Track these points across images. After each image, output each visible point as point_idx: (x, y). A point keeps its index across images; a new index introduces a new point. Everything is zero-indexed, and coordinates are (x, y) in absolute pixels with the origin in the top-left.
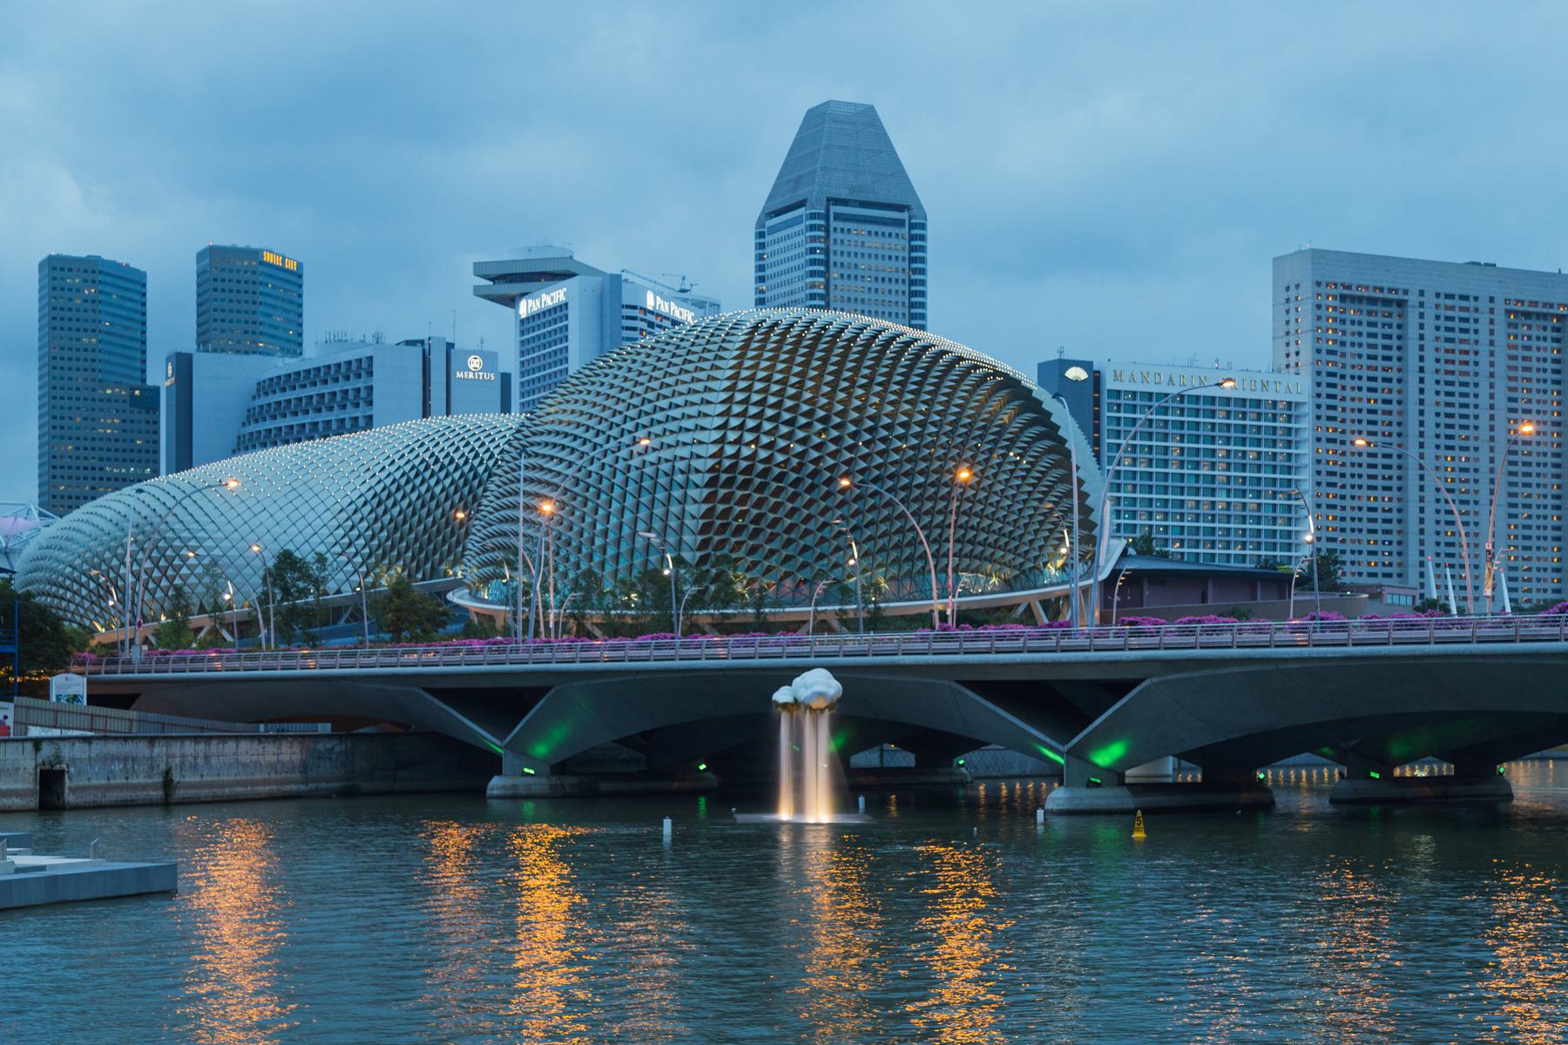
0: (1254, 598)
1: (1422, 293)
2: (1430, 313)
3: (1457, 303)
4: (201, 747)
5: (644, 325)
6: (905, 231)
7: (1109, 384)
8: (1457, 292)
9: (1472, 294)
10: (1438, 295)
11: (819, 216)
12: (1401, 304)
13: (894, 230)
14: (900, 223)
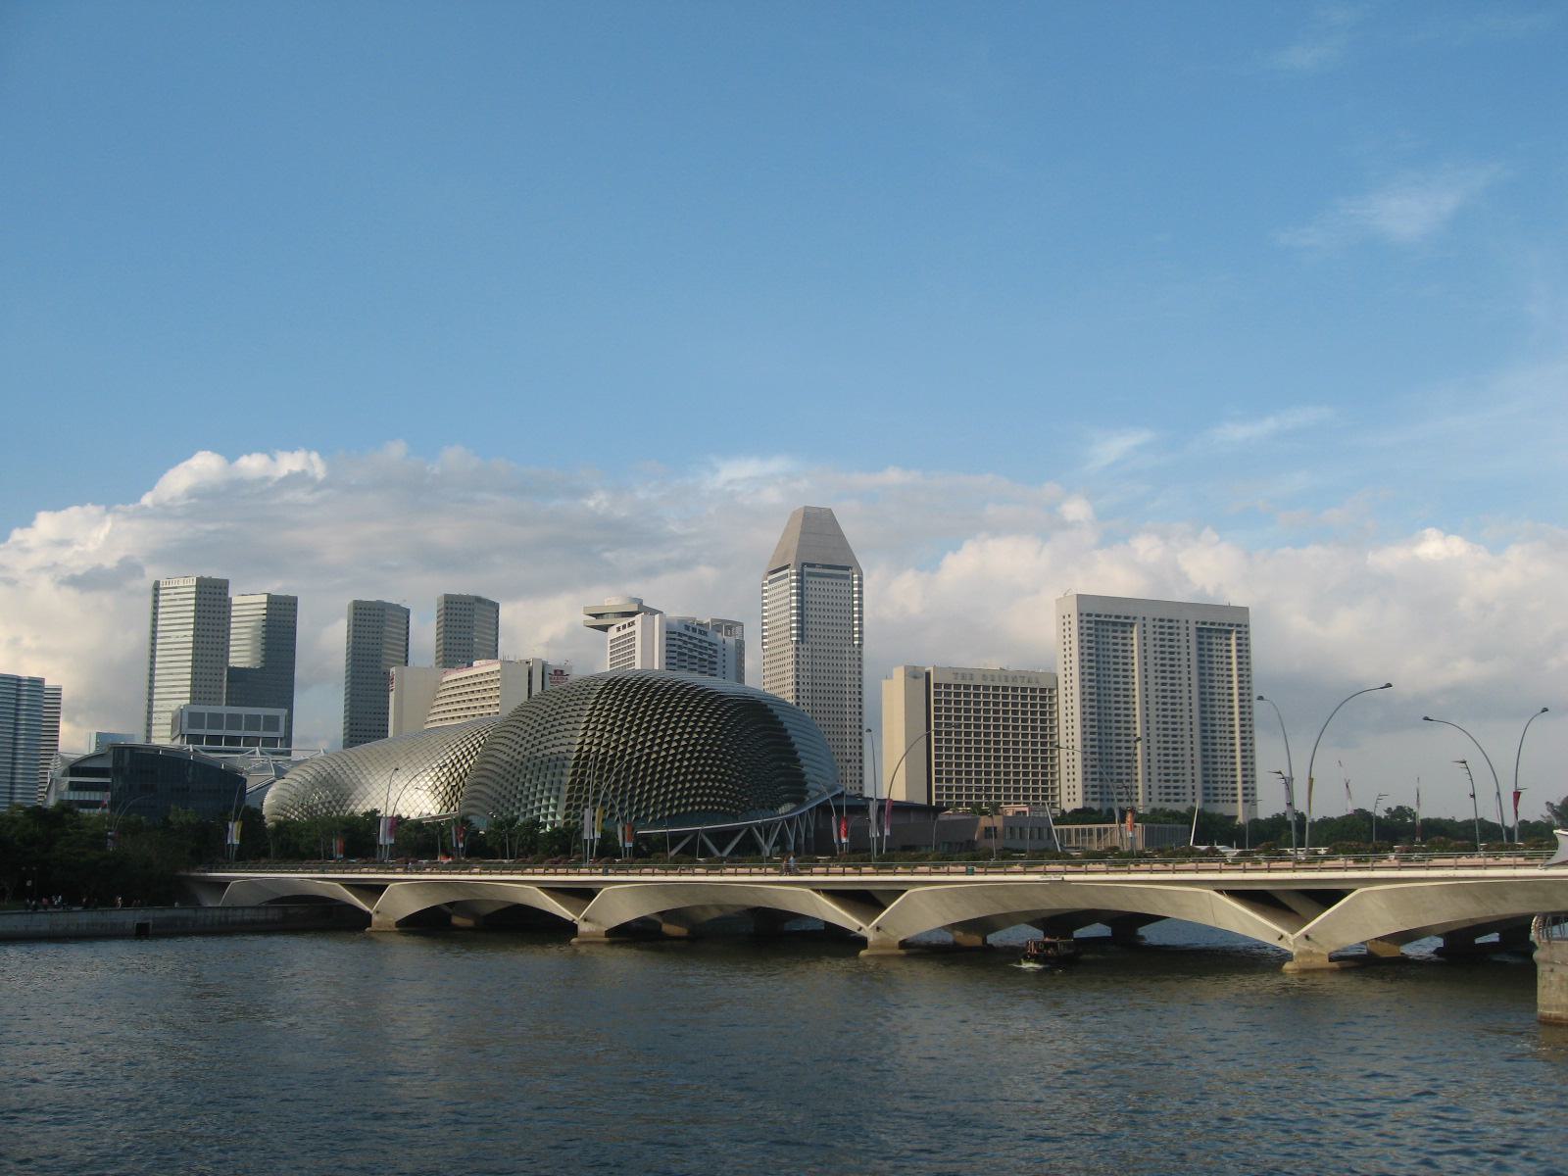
1: (1144, 618)
2: (1149, 629)
4: (224, 912)
5: (680, 643)
8: (1166, 618)
9: (1175, 618)
10: (1154, 620)
13: (843, 581)
14: (847, 577)
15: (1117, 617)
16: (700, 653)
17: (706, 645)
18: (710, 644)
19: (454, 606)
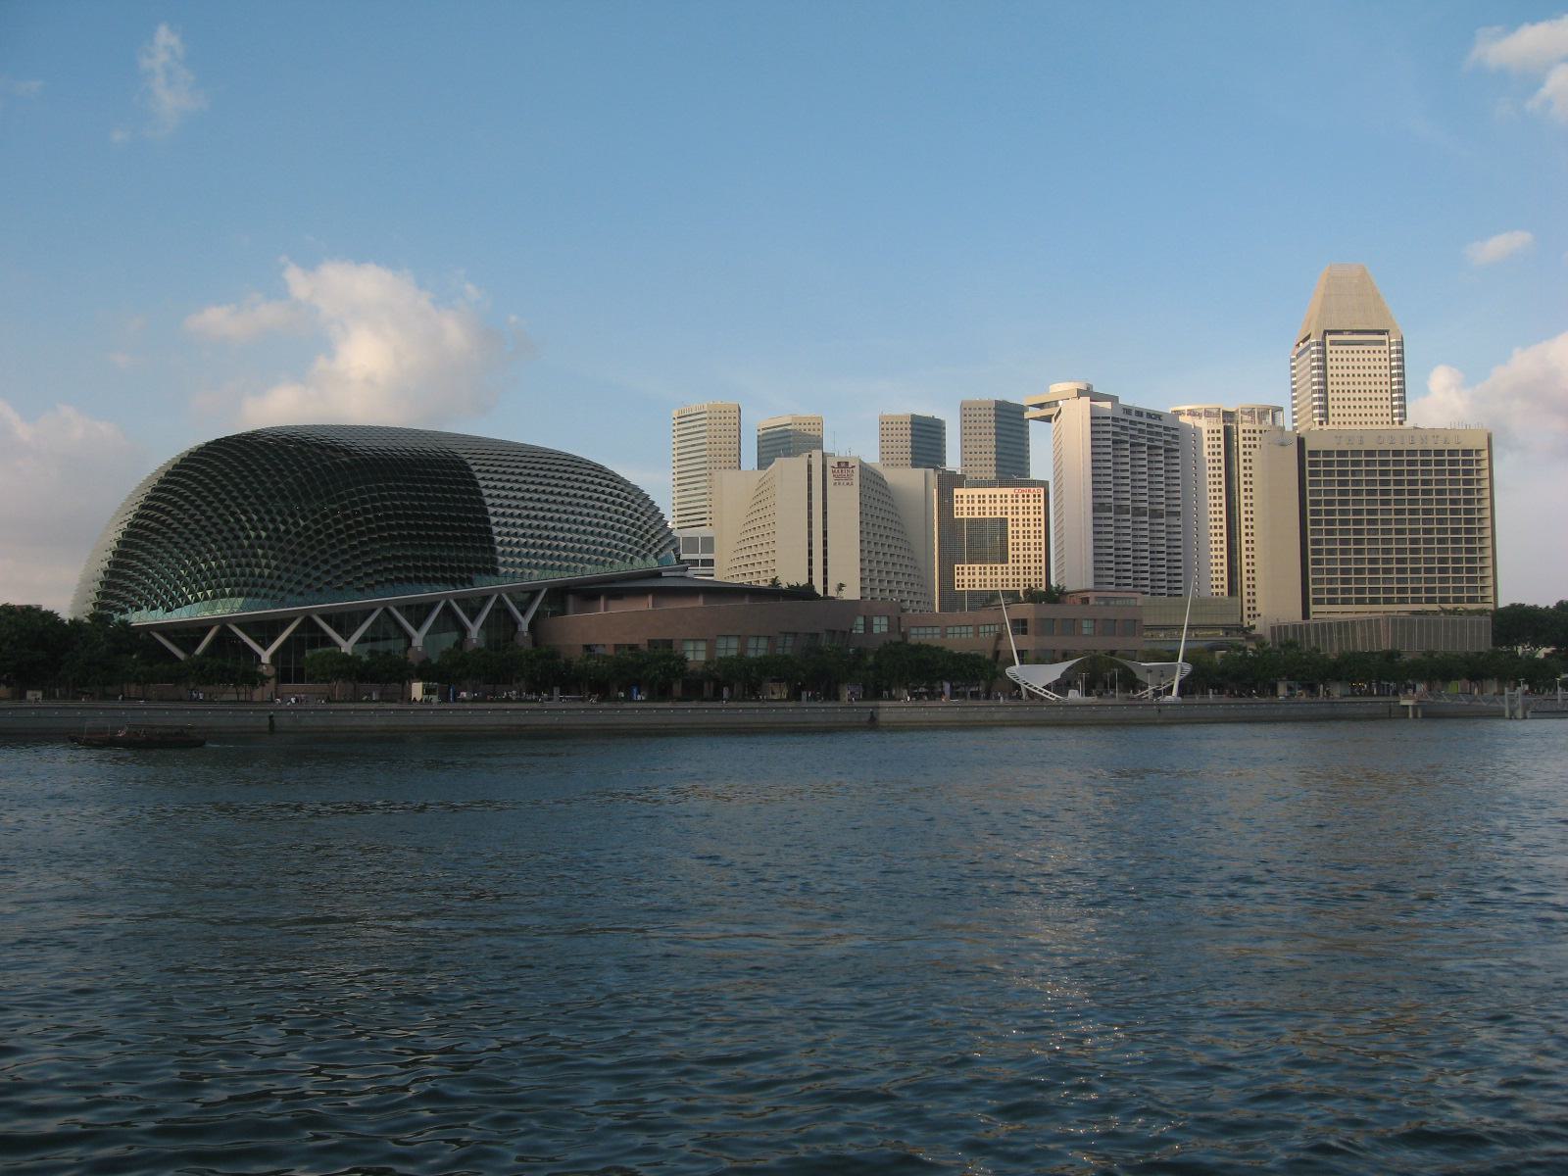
5: (1118, 430)
6: (1386, 348)
7: (1309, 447)
11: (1318, 344)
14: (1382, 343)
16: (1149, 440)
17: (1156, 429)
18: (1166, 428)
19: (973, 412)
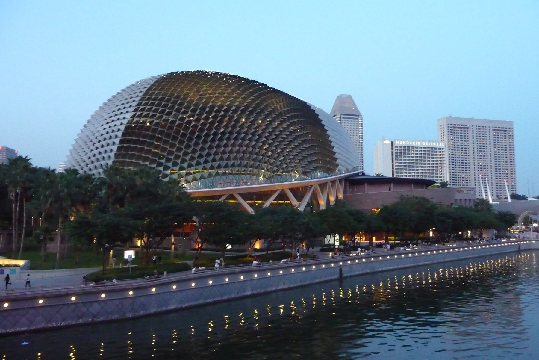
0: (411, 189)
2: (475, 130)
3: (481, 128)
12: (468, 128)
14: (357, 119)
15: (462, 125)
